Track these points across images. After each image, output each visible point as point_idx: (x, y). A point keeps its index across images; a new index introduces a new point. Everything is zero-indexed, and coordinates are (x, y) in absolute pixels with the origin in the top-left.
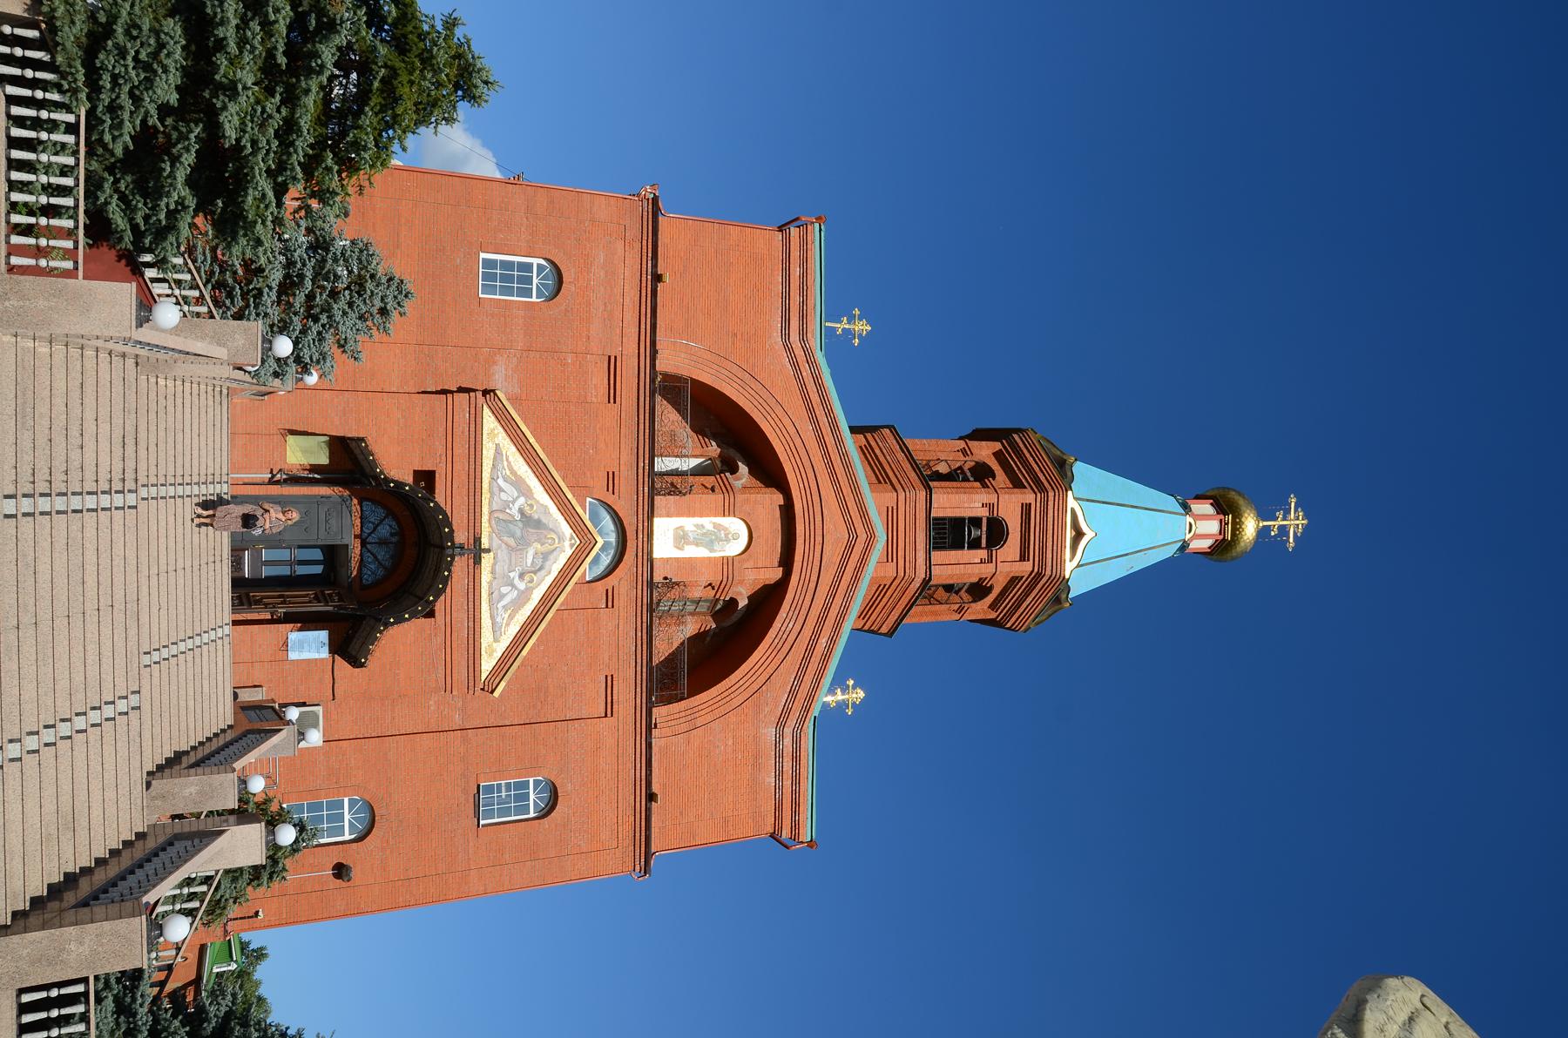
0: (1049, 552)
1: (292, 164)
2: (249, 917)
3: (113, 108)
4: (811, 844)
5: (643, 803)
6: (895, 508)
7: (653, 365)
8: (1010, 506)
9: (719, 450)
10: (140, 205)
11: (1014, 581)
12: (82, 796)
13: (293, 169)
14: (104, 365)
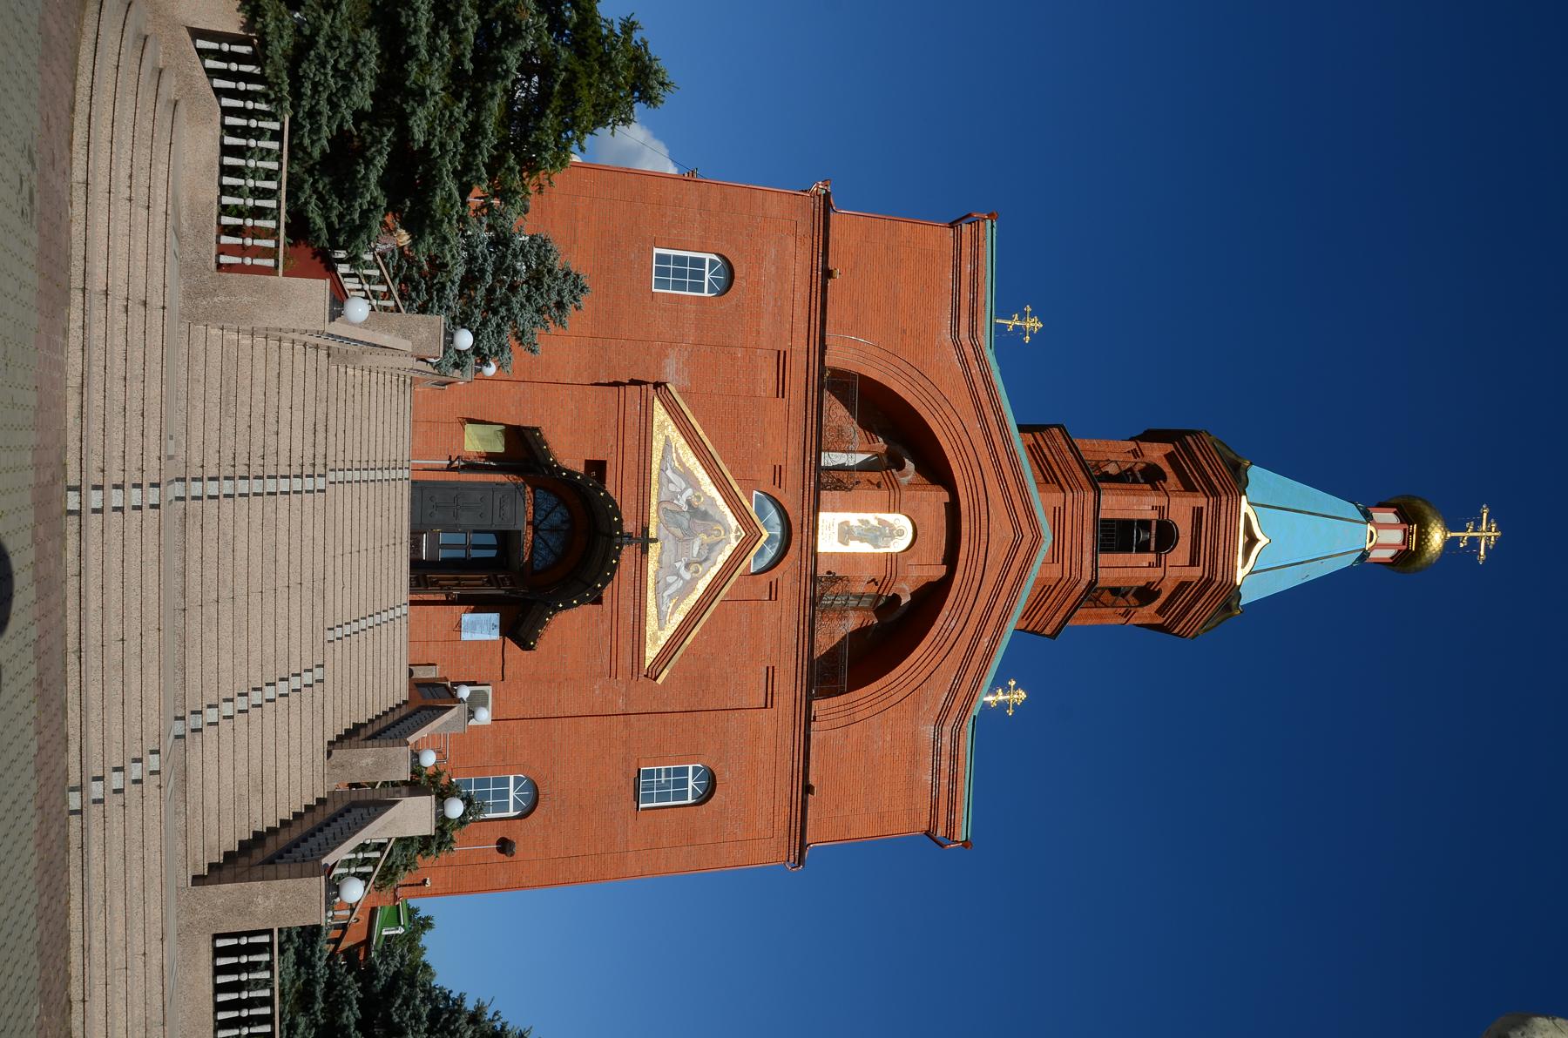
1: (477, 165)
2: (417, 885)
3: (313, 114)
4: (966, 844)
5: (800, 795)
6: (1062, 508)
7: (822, 361)
8: (1181, 510)
9: (886, 446)
10: (335, 204)
11: (1183, 586)
12: (270, 761)
13: (478, 170)
14: (299, 357)
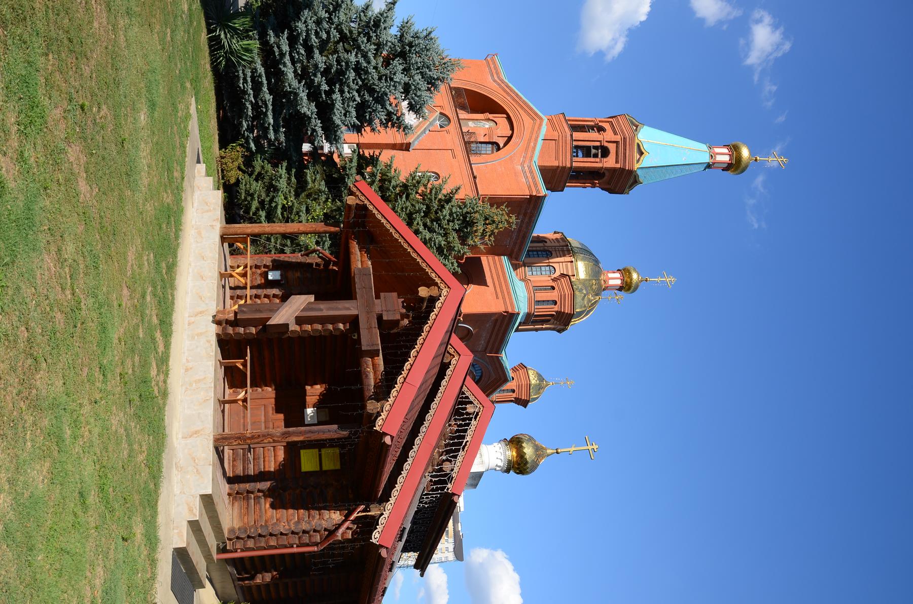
0: (625, 131)
